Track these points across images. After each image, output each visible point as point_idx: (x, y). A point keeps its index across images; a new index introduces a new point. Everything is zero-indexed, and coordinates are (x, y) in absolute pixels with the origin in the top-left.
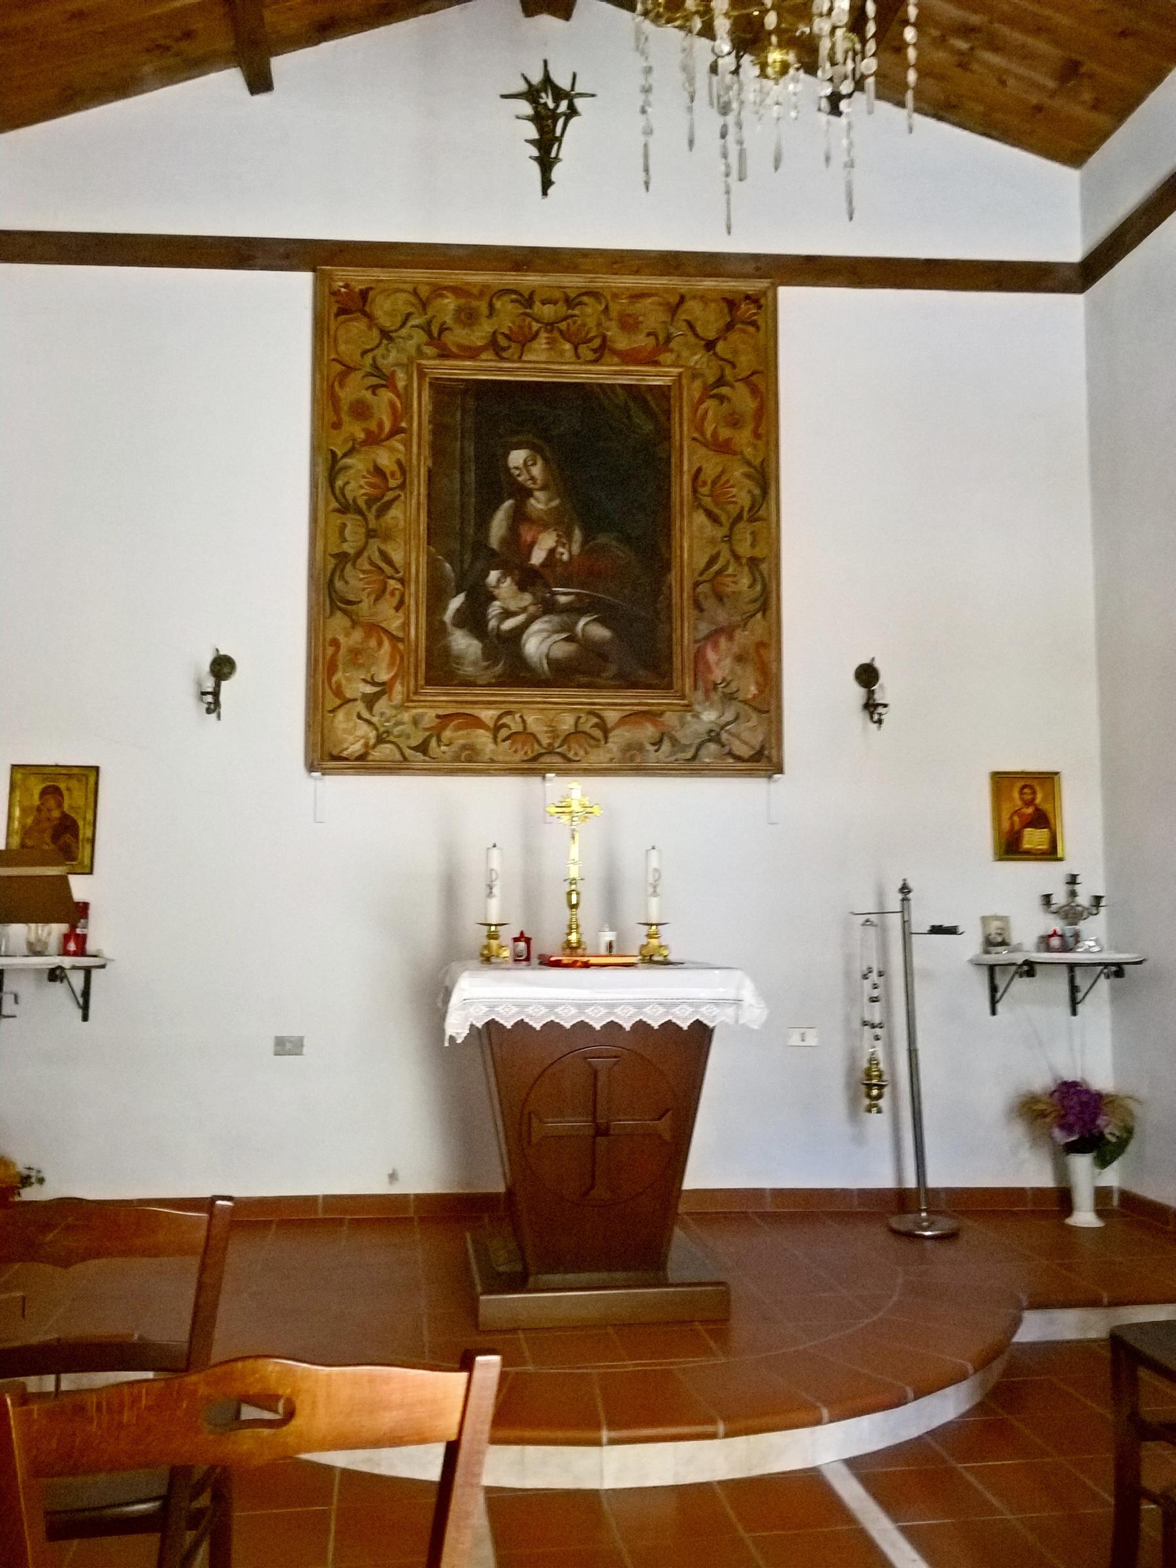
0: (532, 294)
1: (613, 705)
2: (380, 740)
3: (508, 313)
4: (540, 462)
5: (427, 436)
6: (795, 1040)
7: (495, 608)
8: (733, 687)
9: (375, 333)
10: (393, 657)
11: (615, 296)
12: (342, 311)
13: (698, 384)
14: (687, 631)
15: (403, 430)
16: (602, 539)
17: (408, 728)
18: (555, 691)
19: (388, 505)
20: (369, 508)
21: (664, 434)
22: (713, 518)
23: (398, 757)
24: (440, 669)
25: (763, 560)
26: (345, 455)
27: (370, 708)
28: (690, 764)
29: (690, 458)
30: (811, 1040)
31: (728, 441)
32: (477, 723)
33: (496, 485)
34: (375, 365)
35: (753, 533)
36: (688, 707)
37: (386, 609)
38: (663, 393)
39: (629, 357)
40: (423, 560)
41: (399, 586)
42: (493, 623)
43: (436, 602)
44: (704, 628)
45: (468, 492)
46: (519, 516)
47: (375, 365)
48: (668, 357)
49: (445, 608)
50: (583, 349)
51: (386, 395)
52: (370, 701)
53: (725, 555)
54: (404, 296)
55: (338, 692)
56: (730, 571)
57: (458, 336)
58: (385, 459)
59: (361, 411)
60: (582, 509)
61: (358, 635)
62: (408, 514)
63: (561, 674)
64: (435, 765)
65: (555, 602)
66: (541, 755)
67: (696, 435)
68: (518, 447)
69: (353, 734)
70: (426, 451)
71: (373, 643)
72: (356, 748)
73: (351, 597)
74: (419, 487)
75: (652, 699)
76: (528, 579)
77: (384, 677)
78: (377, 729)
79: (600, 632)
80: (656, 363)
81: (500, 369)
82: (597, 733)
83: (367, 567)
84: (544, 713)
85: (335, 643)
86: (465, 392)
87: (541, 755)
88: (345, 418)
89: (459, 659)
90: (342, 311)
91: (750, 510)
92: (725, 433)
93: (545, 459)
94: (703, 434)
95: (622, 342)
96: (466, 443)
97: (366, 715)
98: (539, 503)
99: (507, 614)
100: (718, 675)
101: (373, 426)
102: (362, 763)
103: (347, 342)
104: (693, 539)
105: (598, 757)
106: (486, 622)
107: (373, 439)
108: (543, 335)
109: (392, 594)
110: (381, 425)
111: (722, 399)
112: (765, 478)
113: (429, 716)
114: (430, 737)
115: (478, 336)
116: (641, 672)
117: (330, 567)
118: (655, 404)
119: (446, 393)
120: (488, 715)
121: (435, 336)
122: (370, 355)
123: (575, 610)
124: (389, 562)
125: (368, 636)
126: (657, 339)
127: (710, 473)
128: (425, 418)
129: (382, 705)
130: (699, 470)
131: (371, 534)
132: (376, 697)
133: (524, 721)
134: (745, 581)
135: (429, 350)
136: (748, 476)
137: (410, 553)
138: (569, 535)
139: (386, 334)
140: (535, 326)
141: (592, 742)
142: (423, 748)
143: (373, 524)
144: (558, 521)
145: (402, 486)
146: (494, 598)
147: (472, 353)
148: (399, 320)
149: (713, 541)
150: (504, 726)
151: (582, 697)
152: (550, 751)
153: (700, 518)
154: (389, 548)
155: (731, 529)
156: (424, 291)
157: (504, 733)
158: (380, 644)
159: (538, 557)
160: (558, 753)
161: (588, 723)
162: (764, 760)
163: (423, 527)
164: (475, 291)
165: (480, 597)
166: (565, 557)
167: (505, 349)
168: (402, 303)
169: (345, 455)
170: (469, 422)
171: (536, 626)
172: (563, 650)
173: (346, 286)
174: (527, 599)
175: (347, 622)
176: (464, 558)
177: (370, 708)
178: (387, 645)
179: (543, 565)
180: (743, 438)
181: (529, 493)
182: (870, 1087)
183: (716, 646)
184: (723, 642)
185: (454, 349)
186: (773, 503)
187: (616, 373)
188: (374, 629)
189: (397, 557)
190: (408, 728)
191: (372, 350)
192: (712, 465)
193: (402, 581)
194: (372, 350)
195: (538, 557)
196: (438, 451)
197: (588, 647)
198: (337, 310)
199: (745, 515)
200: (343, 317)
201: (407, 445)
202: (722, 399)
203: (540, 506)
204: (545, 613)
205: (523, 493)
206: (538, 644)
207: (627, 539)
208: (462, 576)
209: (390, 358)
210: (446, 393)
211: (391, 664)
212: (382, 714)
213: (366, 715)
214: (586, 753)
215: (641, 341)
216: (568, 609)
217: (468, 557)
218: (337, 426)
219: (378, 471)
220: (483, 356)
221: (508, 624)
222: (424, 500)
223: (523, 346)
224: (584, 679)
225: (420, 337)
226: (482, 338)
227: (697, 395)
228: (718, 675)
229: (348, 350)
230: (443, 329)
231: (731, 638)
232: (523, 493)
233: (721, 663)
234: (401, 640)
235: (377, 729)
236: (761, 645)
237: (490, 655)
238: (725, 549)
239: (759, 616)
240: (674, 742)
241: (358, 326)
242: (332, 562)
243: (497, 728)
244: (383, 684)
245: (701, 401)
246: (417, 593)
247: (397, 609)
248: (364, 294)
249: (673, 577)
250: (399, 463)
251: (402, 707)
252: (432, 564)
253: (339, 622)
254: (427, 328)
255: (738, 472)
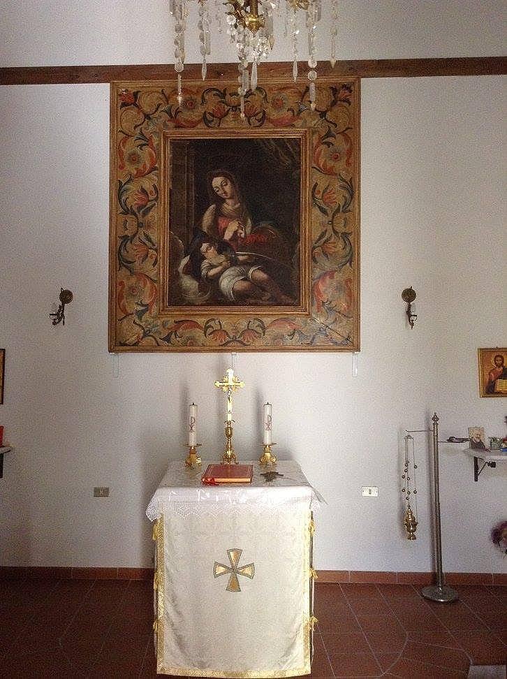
0: (225, 90)
1: (268, 316)
2: (145, 335)
3: (212, 103)
4: (229, 183)
5: (169, 172)
6: (366, 493)
7: (205, 264)
8: (333, 304)
9: (142, 116)
10: (151, 290)
11: (271, 89)
12: (124, 105)
13: (316, 137)
14: (309, 274)
15: (155, 169)
16: (263, 224)
17: (161, 329)
18: (236, 308)
19: (150, 209)
20: (139, 212)
21: (296, 165)
22: (324, 211)
23: (154, 343)
24: (176, 297)
25: (350, 234)
26: (128, 182)
27: (140, 318)
28: (310, 347)
29: (311, 179)
30: (374, 494)
31: (332, 168)
32: (196, 325)
33: (206, 197)
34: (141, 134)
35: (345, 219)
36: (309, 315)
37: (148, 265)
38: (296, 142)
39: (278, 123)
40: (167, 238)
41: (155, 253)
42: (204, 272)
43: (174, 258)
44: (318, 272)
45: (191, 204)
46: (218, 214)
47: (141, 134)
48: (299, 123)
49: (179, 265)
50: (253, 120)
51: (147, 149)
52: (140, 314)
53: (330, 232)
54: (157, 95)
55: (124, 310)
56: (332, 240)
57: (186, 115)
58: (147, 184)
59: (134, 159)
60: (252, 210)
61: (133, 280)
62: (159, 214)
63: (241, 299)
64: (174, 348)
65: (237, 260)
66: (228, 342)
67: (314, 165)
68: (217, 176)
69: (132, 331)
70: (168, 180)
71: (141, 285)
72: (133, 339)
73: (130, 260)
74: (165, 198)
75: (288, 311)
76: (223, 247)
77: (147, 301)
78: (143, 329)
79: (261, 275)
80: (293, 126)
81: (209, 133)
82: (259, 330)
83: (138, 243)
84: (228, 320)
85: (122, 283)
86: (189, 147)
87: (228, 342)
88: (127, 163)
89: (186, 291)
90: (124, 105)
91: (343, 207)
92: (330, 163)
93: (232, 182)
94: (318, 165)
95: (274, 115)
96: (190, 175)
97: (137, 321)
98: (229, 206)
99: (212, 267)
100: (325, 297)
101: (141, 167)
102: (136, 347)
103: (126, 121)
104: (312, 223)
105: (259, 343)
106: (200, 271)
107: (141, 174)
108: (231, 112)
109: (151, 257)
110: (145, 166)
111: (329, 144)
112: (352, 189)
113: (171, 322)
114: (171, 333)
115: (196, 115)
116: (283, 297)
117: (119, 244)
118: (291, 149)
119: (178, 146)
120: (201, 321)
121: (173, 115)
122: (139, 128)
123: (247, 264)
124: (150, 240)
125: (139, 280)
126: (293, 111)
127: (321, 187)
128: (168, 162)
129: (146, 316)
130: (316, 185)
131: (140, 225)
132: (143, 312)
133: (220, 325)
134: (340, 245)
135: (171, 124)
136: (343, 187)
137: (160, 234)
138: (245, 223)
139: (147, 116)
140: (227, 108)
141: (257, 335)
142: (168, 339)
143: (141, 220)
144: (239, 216)
145: (156, 199)
146: (204, 258)
147: (193, 125)
148: (155, 107)
149: (322, 224)
150: (210, 326)
151: (250, 310)
152: (234, 340)
153: (316, 211)
154: (149, 233)
155: (333, 217)
156: (167, 92)
157: (210, 330)
158: (145, 285)
159: (228, 236)
160: (239, 341)
161: (255, 325)
162: (351, 343)
163: (167, 221)
164: (194, 90)
165: (197, 258)
166: (243, 235)
167: (210, 122)
168: (155, 98)
169: (128, 182)
170: (192, 163)
171: (227, 273)
172: (241, 285)
173: (126, 91)
174: (222, 258)
175: (129, 273)
176: (189, 234)
177: (140, 318)
178: (149, 284)
179: (230, 240)
180: (340, 166)
181: (223, 200)
182: (409, 527)
183: (324, 280)
184: (328, 279)
185: (184, 123)
186: (356, 201)
187: (270, 132)
188: (143, 276)
189: (154, 238)
190: (161, 329)
191: (140, 125)
192: (322, 181)
193: (156, 250)
194: (140, 125)
195: (228, 236)
196: (175, 180)
197: (256, 285)
198: (123, 103)
199: (341, 210)
200: (124, 108)
201: (158, 176)
202: (329, 144)
203: (230, 207)
204: (231, 266)
205: (220, 201)
206: (229, 282)
207: (276, 225)
208: (188, 246)
209: (150, 129)
210: (178, 146)
211: (151, 295)
212: (147, 321)
213: (137, 321)
214: (254, 340)
215: (285, 114)
216: (244, 263)
217: (191, 236)
218: (122, 167)
219: (143, 191)
220: (199, 126)
221: (212, 272)
222: (167, 206)
223: (220, 119)
224: (252, 301)
225: (165, 116)
226: (199, 116)
227: (315, 143)
228: (325, 297)
229: (126, 126)
230: (177, 112)
231: (332, 277)
232: (220, 201)
233: (327, 289)
234: (155, 281)
235: (143, 329)
236: (349, 280)
237: (202, 289)
238: (330, 227)
239: (348, 264)
240: (301, 334)
241: (133, 112)
242: (120, 241)
243: (207, 328)
244: (145, 305)
245: (317, 147)
246: (164, 257)
247: (154, 265)
248: (135, 94)
249: (301, 245)
250: (154, 186)
251: (156, 317)
252: (173, 242)
253: (124, 272)
254: (169, 112)
255: (337, 185)
